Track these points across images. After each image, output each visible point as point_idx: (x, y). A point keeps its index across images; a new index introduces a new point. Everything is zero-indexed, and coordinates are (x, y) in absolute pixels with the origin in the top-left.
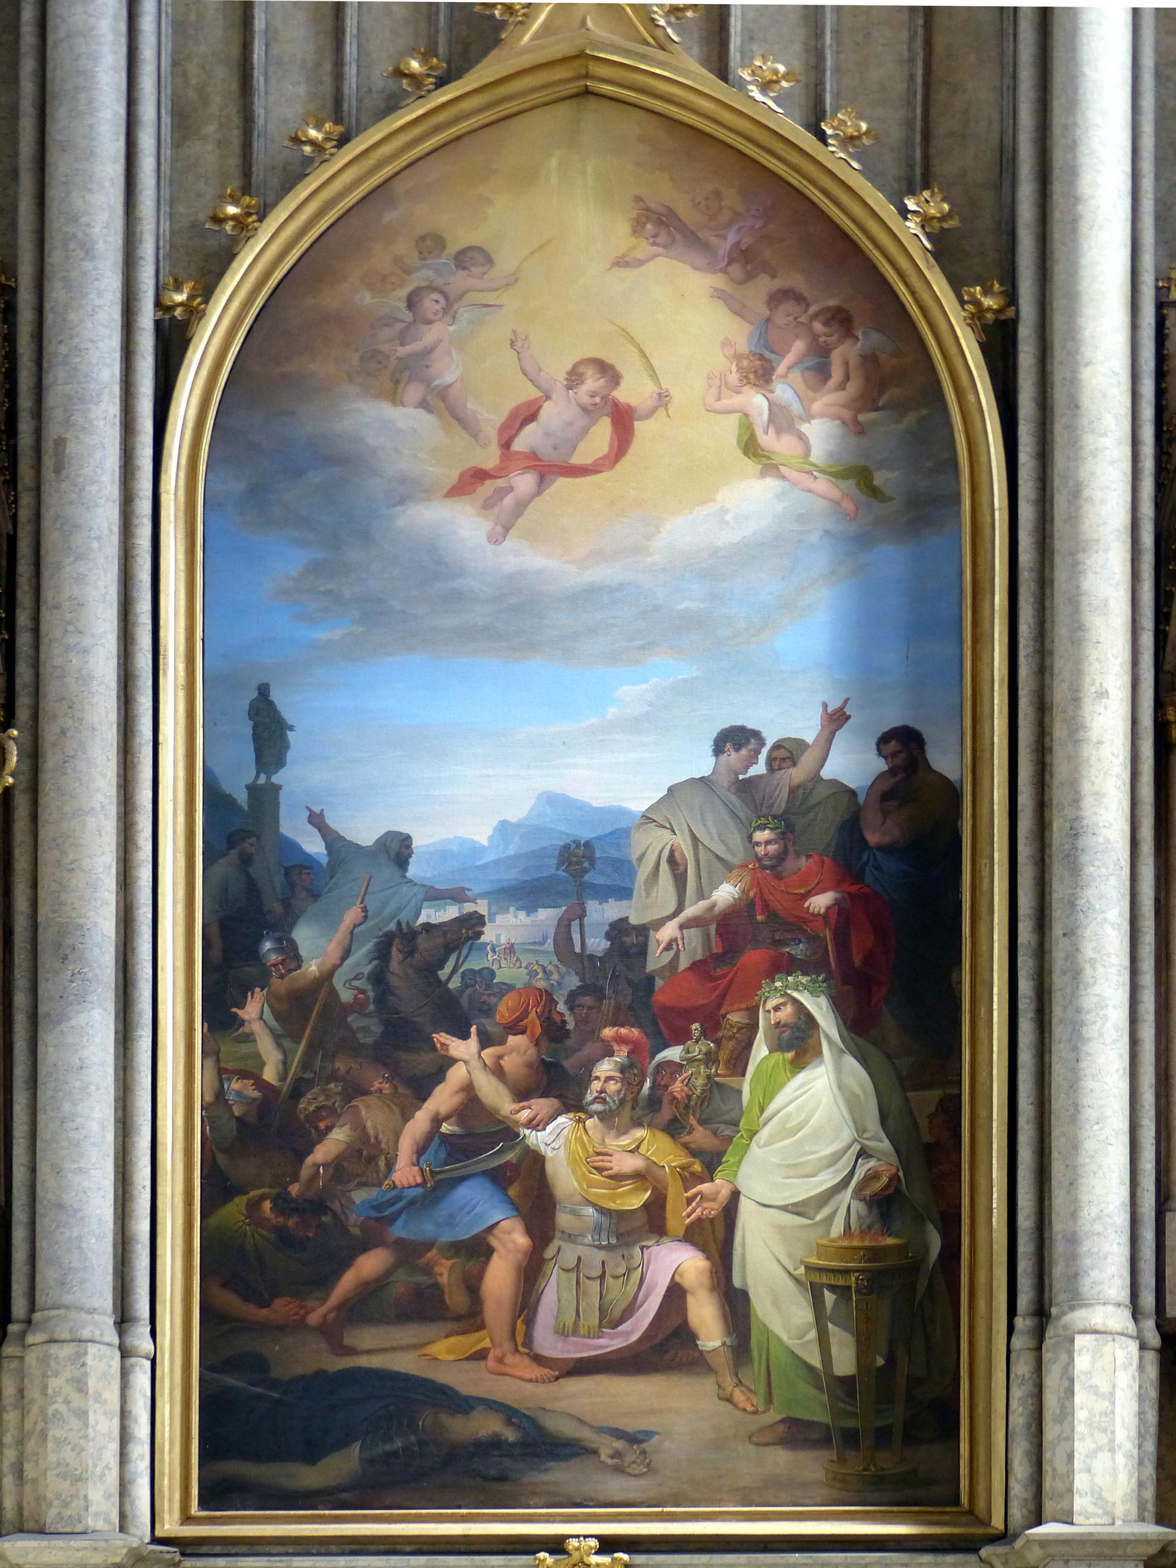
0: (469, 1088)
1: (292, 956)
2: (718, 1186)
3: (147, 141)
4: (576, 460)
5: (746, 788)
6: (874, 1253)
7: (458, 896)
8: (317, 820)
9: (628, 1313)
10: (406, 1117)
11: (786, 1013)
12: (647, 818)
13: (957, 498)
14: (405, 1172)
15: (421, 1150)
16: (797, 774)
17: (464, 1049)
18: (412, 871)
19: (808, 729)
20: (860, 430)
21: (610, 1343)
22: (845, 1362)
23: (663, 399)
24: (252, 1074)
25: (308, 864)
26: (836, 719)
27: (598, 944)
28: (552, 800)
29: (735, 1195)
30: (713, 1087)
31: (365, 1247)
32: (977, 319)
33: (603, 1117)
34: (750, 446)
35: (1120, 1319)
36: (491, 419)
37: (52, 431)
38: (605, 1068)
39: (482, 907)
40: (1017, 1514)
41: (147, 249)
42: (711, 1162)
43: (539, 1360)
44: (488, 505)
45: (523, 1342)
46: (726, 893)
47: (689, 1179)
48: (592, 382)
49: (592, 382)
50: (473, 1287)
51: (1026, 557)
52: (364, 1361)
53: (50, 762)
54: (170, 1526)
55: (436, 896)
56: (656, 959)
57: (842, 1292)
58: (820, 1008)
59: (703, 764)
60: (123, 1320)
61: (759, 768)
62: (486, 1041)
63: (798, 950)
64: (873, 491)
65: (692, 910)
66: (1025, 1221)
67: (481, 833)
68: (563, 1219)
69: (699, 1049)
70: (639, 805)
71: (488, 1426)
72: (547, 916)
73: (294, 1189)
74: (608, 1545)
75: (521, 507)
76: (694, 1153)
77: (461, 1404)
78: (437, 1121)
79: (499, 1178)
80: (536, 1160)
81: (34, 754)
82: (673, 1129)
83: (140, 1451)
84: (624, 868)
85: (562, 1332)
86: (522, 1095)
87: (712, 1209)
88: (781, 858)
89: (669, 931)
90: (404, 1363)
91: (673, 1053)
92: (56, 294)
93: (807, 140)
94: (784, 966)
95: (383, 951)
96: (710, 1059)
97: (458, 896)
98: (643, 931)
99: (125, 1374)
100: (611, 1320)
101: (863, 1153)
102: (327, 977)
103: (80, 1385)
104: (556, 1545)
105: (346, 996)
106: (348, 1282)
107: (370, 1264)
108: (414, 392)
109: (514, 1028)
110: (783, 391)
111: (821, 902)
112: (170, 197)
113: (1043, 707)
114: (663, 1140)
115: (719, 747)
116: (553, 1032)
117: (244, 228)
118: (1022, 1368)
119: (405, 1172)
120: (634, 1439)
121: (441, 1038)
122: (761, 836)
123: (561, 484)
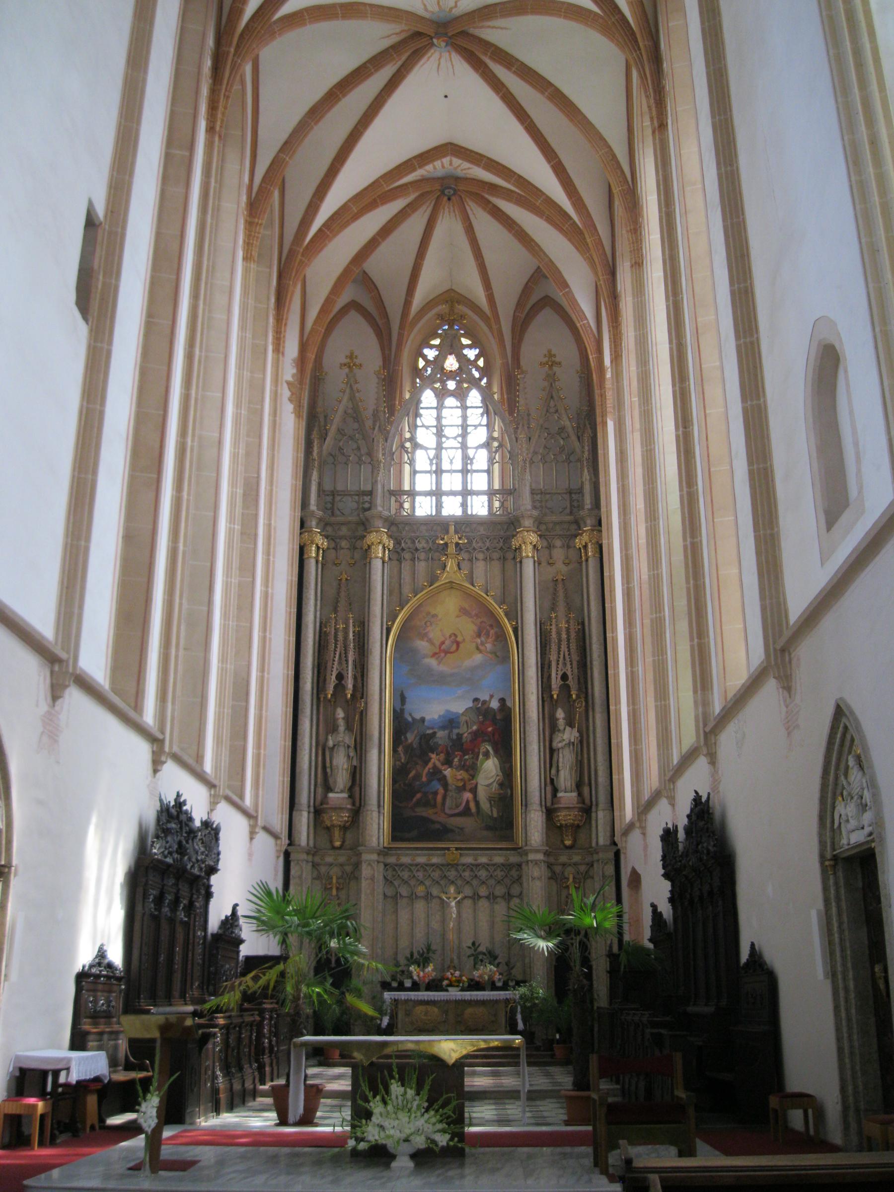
0: (434, 763)
1: (406, 738)
2: (474, 781)
3: (385, 597)
4: (451, 650)
5: (478, 709)
6: (500, 794)
7: (432, 728)
8: (410, 715)
9: (461, 804)
10: (424, 768)
11: (485, 750)
12: (463, 714)
13: (509, 657)
14: (424, 779)
15: (427, 775)
16: (486, 706)
17: (433, 756)
18: (426, 723)
19: (487, 698)
20: (494, 645)
21: (457, 811)
22: (495, 815)
23: (464, 639)
24: (400, 760)
25: (409, 722)
26: (492, 696)
27: (455, 737)
28: (447, 711)
29: (477, 784)
30: (473, 763)
31: (418, 792)
32: (512, 625)
33: (456, 769)
34: (478, 648)
35: (538, 808)
36: (437, 643)
37: (370, 647)
38: (456, 760)
39: (436, 730)
40: (524, 844)
41: (385, 616)
42: (473, 777)
43: (445, 814)
44: (437, 659)
45: (443, 810)
46: (475, 728)
47: (470, 780)
48: (453, 637)
49: (453, 637)
50: (435, 800)
51: (520, 668)
52: (418, 814)
53: (369, 705)
54: (386, 845)
55: (429, 728)
56: (464, 740)
57: (494, 801)
58: (490, 748)
59: (470, 704)
60: (379, 806)
61: (480, 705)
62: (437, 755)
63: (486, 738)
64: (497, 656)
65: (469, 731)
66: (523, 789)
67: (436, 717)
68: (450, 788)
69: (471, 756)
70: (461, 712)
71: (437, 826)
72: (447, 732)
73: (407, 782)
74: (457, 849)
75: (442, 659)
76: (471, 775)
77: (433, 822)
78: (429, 769)
79: (439, 780)
80: (445, 777)
81: (366, 703)
82: (467, 771)
83: (381, 831)
84: (459, 723)
85: (450, 809)
86: (443, 764)
87: (473, 786)
88: (483, 721)
89: (466, 735)
90: (424, 814)
91: (467, 757)
92: (371, 624)
93: (485, 595)
94: (485, 741)
95: (421, 739)
96: (473, 758)
97: (432, 728)
98: (462, 735)
99: (379, 816)
100: (457, 806)
101: (498, 775)
102: (412, 743)
103: (372, 819)
104: (448, 849)
105: (415, 746)
106: (415, 799)
107: (419, 796)
108: (425, 639)
109: (442, 752)
110: (483, 639)
111: (490, 729)
112: (388, 606)
113: (524, 695)
114: (466, 773)
115: (473, 701)
116: (448, 754)
117: (400, 611)
118: (524, 816)
119: (424, 779)
120: (462, 829)
121: (430, 754)
122: (480, 717)
123: (449, 655)
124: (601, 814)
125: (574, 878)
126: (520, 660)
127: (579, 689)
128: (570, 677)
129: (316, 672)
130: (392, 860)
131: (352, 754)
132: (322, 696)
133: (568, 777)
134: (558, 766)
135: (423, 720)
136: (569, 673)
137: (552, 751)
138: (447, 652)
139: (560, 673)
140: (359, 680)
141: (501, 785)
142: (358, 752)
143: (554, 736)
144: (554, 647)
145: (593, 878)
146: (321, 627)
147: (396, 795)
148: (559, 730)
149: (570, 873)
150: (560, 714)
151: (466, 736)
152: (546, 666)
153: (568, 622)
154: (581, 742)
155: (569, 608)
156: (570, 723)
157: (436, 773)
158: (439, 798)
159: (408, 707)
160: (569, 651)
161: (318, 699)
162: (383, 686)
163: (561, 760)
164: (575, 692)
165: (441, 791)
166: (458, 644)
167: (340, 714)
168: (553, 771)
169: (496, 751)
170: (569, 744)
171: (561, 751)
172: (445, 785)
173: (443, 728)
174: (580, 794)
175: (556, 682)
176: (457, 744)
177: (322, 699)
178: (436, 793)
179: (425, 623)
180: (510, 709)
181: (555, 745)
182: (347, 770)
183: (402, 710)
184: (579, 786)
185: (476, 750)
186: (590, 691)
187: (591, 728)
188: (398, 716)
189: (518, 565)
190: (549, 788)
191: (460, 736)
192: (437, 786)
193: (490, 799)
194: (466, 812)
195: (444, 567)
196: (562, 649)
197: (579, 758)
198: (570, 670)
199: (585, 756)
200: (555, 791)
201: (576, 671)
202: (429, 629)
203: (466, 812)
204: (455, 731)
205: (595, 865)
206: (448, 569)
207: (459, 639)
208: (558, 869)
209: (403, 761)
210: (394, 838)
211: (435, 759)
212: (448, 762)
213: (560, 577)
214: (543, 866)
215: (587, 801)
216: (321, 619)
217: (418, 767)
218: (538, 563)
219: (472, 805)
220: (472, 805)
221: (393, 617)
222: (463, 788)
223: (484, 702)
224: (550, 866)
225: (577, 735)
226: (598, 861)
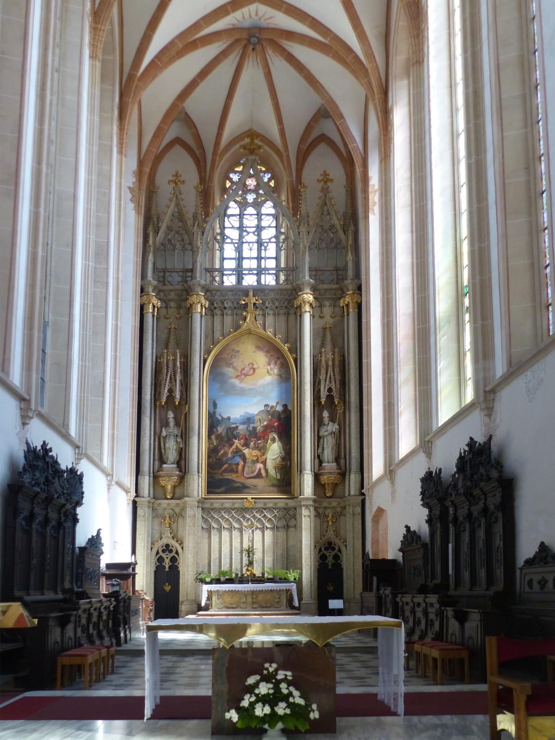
0: (237, 446)
1: (217, 431)
2: (264, 457)
3: (202, 339)
6: (282, 465)
7: (236, 424)
8: (220, 415)
12: (257, 415)
14: (230, 455)
15: (231, 453)
17: (236, 441)
18: (231, 421)
22: (279, 477)
23: (258, 367)
24: (213, 444)
25: (219, 420)
27: (251, 429)
32: (293, 358)
33: (252, 449)
34: (268, 372)
36: (240, 369)
38: (252, 443)
42: (264, 454)
46: (265, 423)
47: (262, 456)
49: (251, 365)
50: (237, 469)
54: (203, 496)
55: (233, 424)
56: (258, 431)
58: (276, 436)
59: (263, 408)
60: (198, 472)
61: (269, 409)
63: (273, 430)
68: (247, 461)
70: (256, 413)
71: (239, 485)
72: (245, 426)
74: (252, 498)
75: (243, 379)
79: (240, 456)
80: (244, 454)
81: (189, 408)
82: (259, 450)
84: (254, 420)
86: (243, 446)
89: (259, 428)
90: (229, 477)
91: (260, 442)
94: (272, 431)
95: (227, 430)
98: (256, 428)
100: (253, 472)
104: (246, 498)
107: (226, 466)
110: (272, 366)
111: (276, 424)
116: (246, 439)
119: (230, 455)
124: (353, 476)
125: (332, 516)
126: (299, 379)
127: (340, 398)
128: (334, 390)
129: (153, 388)
130: (207, 505)
131: (179, 440)
132: (158, 404)
133: (330, 453)
134: (323, 447)
135: (229, 418)
136: (333, 388)
137: (319, 438)
138: (246, 375)
139: (327, 387)
140: (184, 393)
141: (283, 459)
142: (184, 438)
143: (321, 429)
144: (323, 371)
145: (345, 515)
146: (156, 359)
147: (210, 466)
148: (324, 425)
149: (330, 513)
150: (326, 414)
151: (259, 429)
152: (317, 384)
153: (333, 354)
154: (340, 432)
155: (334, 346)
156: (332, 419)
157: (238, 452)
158: (240, 467)
159: (218, 410)
160: (334, 373)
161: (155, 405)
162: (201, 397)
163: (325, 443)
164: (338, 400)
165: (242, 463)
166: (254, 370)
167: (171, 415)
168: (320, 450)
169: (280, 438)
170: (331, 433)
171: (325, 438)
172: (244, 459)
173: (243, 423)
174: (338, 464)
175: (324, 394)
176: (253, 433)
177: (158, 405)
178: (238, 464)
179: (231, 356)
180: (290, 411)
181: (321, 433)
182: (176, 450)
183: (214, 413)
184: (337, 459)
185: (266, 437)
186: (347, 399)
187: (347, 423)
188: (211, 416)
189: (298, 318)
190: (317, 461)
191: (255, 429)
192: (238, 459)
193: (275, 468)
194: (259, 475)
195: (245, 319)
196: (329, 372)
197: (338, 442)
198: (334, 385)
199: (342, 440)
200: (321, 462)
201: (338, 386)
202: (234, 360)
203: (259, 475)
204: (252, 425)
205: (347, 508)
206: (248, 320)
207: (255, 366)
208: (321, 511)
209: (215, 444)
210: (209, 492)
211: (237, 443)
212: (247, 445)
213: (328, 326)
214: (312, 509)
215: (343, 468)
216: (156, 354)
217: (226, 449)
218: (313, 316)
219: (263, 472)
220: (263, 472)
221: (208, 352)
222: (257, 461)
223: (272, 407)
224: (316, 509)
225: (337, 427)
226: (349, 505)
